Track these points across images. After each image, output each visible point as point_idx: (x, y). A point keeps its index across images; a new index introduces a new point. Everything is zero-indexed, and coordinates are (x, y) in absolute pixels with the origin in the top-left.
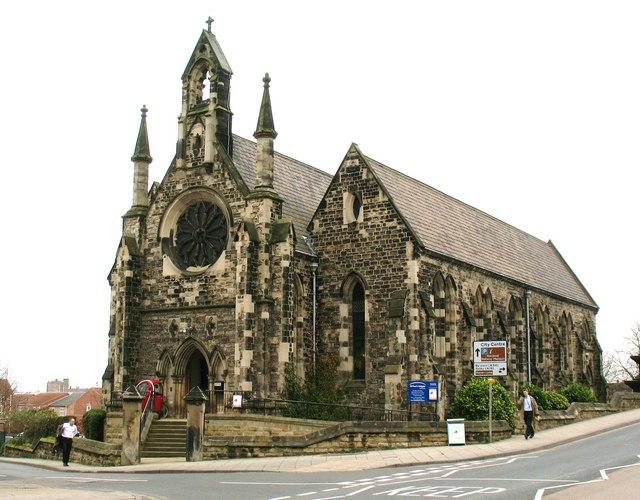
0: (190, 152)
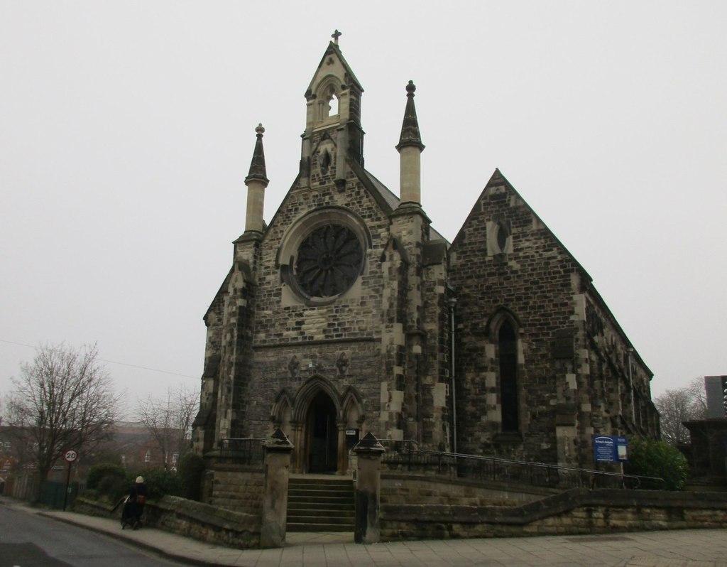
0: (317, 170)
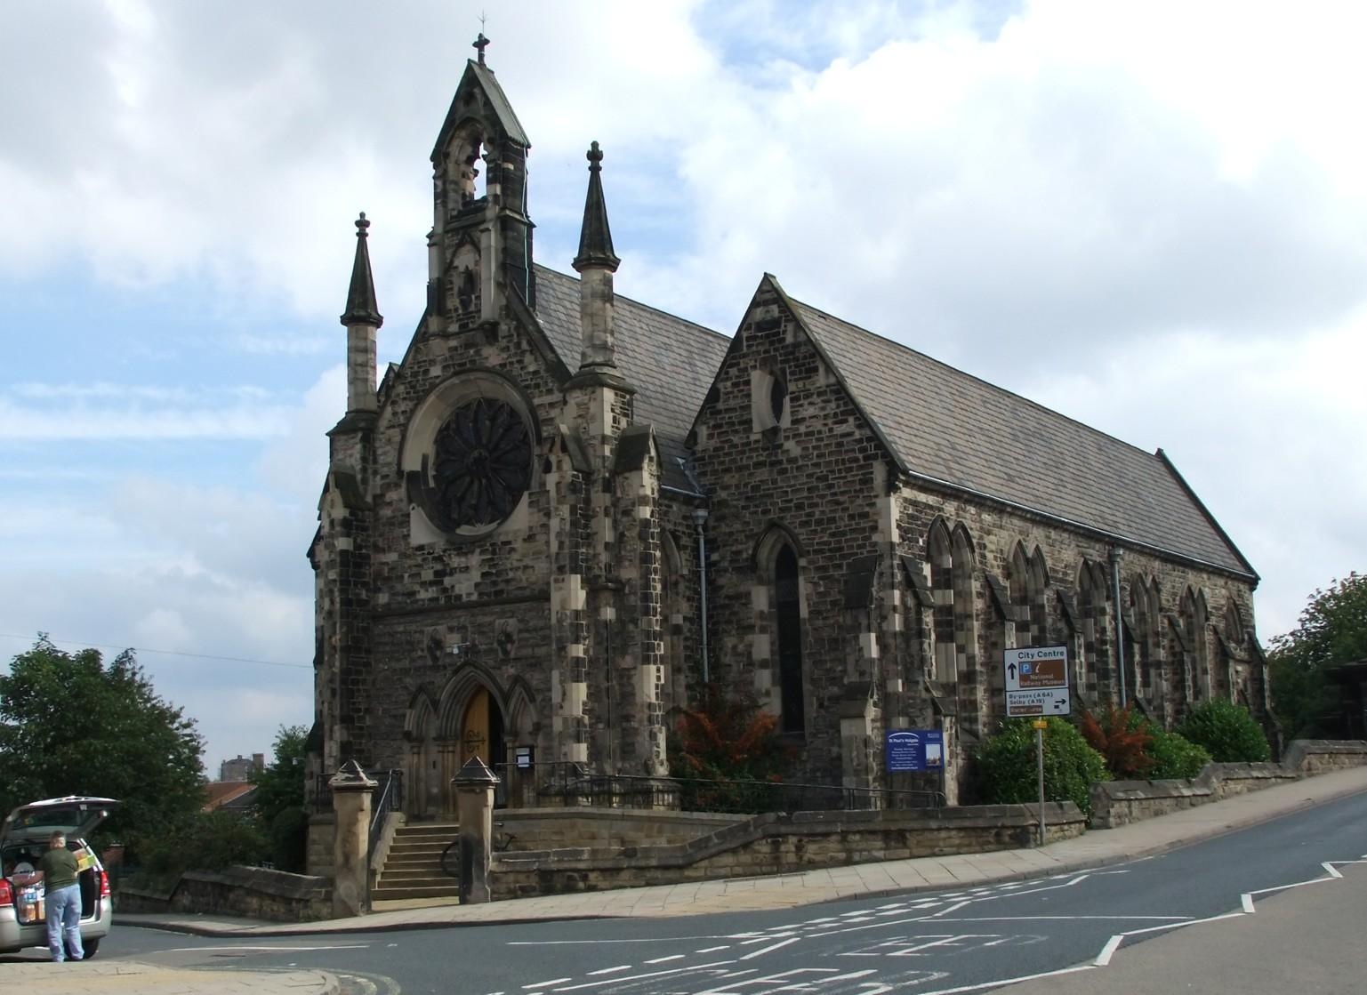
0: (453, 302)
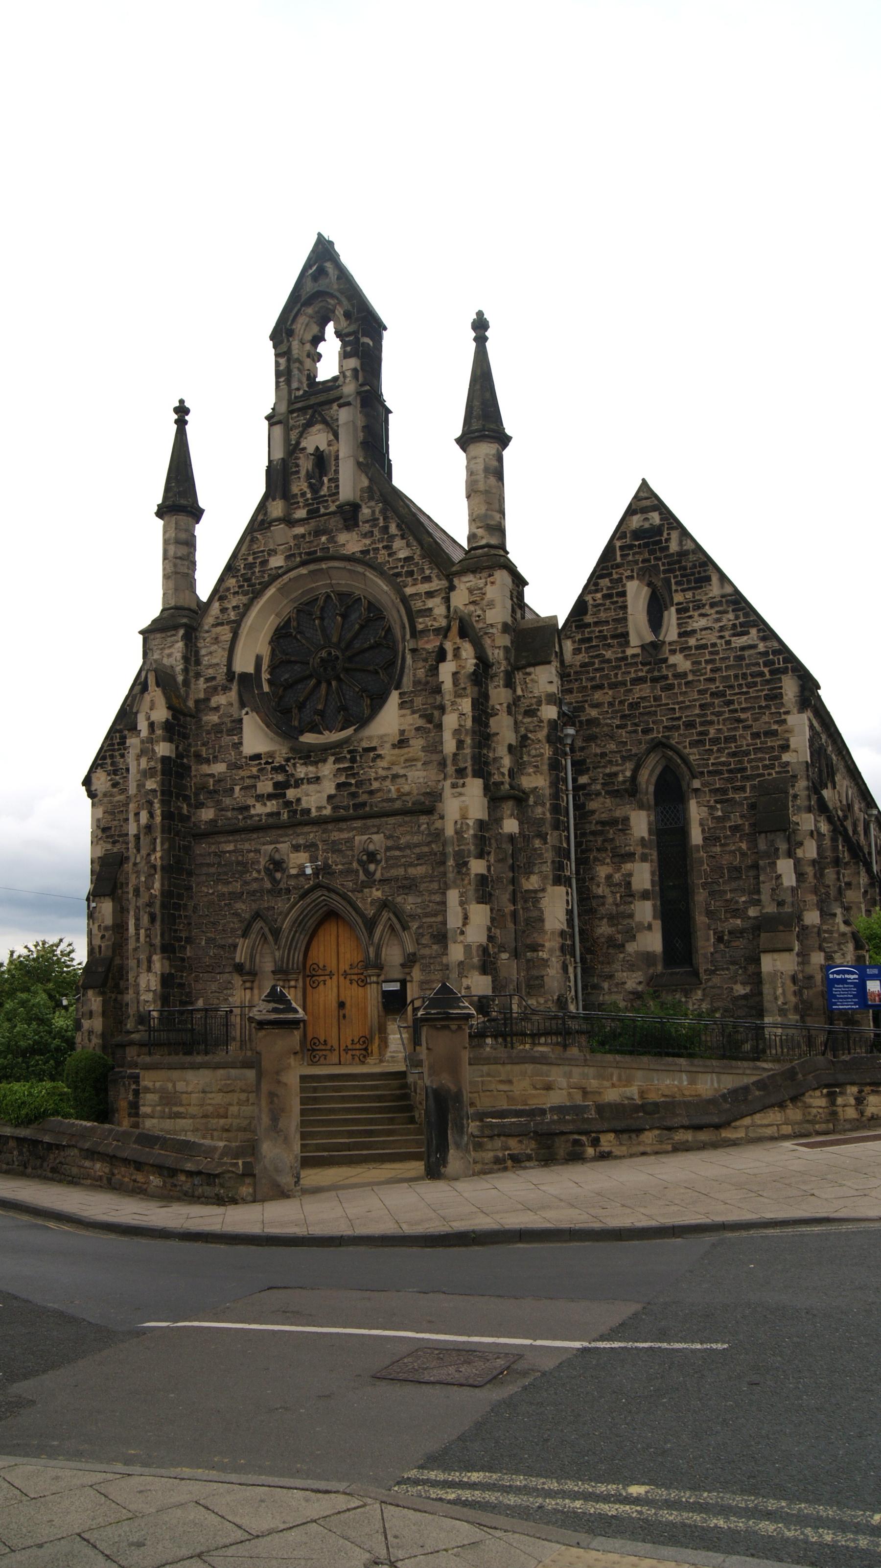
0: (300, 486)
